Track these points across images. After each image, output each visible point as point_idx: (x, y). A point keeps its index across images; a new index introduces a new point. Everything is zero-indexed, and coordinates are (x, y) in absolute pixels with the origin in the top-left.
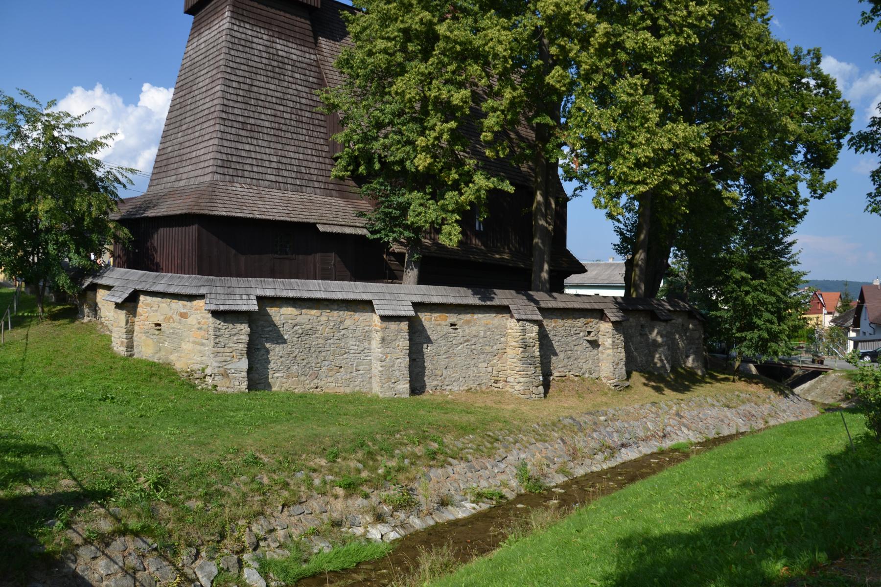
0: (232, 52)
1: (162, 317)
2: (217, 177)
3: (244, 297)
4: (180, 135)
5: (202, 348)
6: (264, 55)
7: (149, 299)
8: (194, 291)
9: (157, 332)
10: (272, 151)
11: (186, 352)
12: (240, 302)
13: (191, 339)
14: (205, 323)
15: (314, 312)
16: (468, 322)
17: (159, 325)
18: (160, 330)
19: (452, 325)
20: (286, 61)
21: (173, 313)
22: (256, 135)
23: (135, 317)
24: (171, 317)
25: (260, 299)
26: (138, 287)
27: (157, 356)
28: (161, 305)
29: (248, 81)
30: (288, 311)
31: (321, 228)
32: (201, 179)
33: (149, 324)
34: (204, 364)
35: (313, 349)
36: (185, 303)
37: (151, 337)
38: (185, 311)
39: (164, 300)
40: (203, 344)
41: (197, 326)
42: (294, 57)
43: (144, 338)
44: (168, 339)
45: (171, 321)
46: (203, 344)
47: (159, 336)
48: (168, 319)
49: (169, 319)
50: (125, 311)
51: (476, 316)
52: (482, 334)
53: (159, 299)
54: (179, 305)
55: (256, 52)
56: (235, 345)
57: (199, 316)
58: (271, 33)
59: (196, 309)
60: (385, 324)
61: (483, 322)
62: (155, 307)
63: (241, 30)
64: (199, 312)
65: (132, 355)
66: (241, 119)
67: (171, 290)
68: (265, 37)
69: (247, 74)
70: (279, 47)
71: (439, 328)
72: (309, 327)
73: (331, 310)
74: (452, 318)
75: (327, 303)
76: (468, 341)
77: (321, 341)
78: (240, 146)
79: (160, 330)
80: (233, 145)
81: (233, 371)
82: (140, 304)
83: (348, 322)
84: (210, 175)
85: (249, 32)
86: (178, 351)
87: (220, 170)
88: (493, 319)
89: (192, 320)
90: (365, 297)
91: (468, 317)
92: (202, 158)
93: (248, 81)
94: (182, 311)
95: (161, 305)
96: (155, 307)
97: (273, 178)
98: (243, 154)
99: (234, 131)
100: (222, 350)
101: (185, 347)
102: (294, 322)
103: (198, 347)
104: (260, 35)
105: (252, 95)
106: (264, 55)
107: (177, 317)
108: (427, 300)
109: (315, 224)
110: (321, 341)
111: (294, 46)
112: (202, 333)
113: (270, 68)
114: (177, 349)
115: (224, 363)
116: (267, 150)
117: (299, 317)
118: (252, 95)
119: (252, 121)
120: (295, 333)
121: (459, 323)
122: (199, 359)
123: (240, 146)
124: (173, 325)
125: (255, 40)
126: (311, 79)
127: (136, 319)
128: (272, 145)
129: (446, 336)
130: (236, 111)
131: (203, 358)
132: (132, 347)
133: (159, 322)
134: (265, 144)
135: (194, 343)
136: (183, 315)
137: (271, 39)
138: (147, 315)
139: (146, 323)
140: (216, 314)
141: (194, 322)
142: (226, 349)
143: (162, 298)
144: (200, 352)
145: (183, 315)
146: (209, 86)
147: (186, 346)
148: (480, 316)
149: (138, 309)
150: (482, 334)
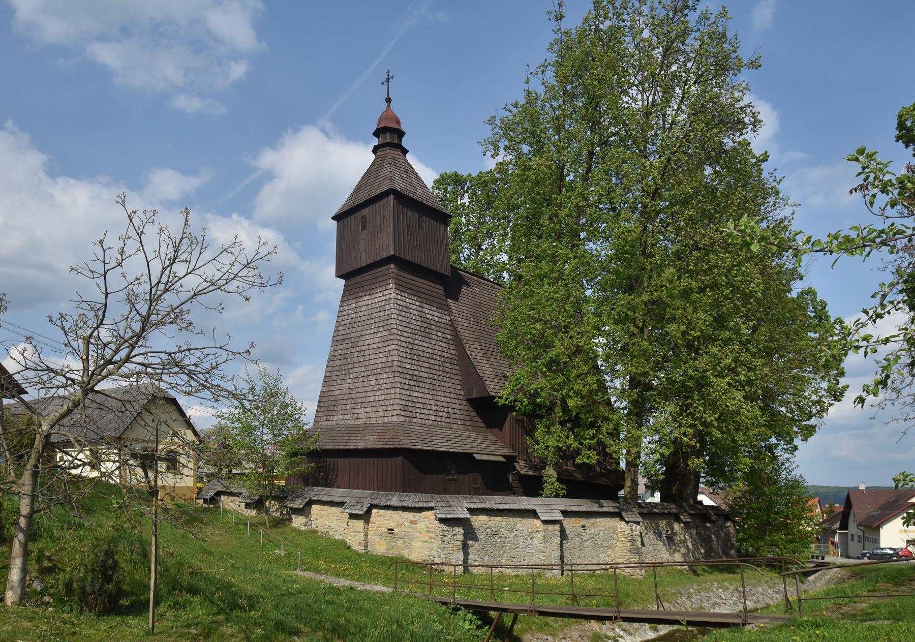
0: (400, 318)
2: (401, 418)
3: (460, 508)
4: (348, 381)
5: (430, 545)
6: (418, 318)
7: (381, 512)
8: (424, 505)
9: (390, 535)
10: (431, 397)
12: (458, 512)
13: (421, 539)
15: (499, 519)
16: (593, 525)
17: (393, 530)
19: (583, 526)
20: (432, 322)
22: (420, 384)
24: (402, 524)
25: (469, 509)
27: (391, 552)
28: (393, 515)
29: (411, 341)
30: (483, 518)
31: (478, 457)
32: (390, 419)
35: (497, 545)
40: (430, 542)
42: (436, 319)
45: (403, 526)
46: (430, 542)
48: (400, 525)
49: (401, 525)
51: (598, 520)
52: (602, 533)
53: (392, 511)
54: (410, 516)
55: (414, 317)
57: (427, 523)
58: (420, 300)
59: (425, 518)
60: (546, 526)
61: (602, 524)
62: (388, 517)
63: (403, 299)
65: (367, 552)
66: (410, 372)
67: (405, 504)
68: (417, 303)
69: (410, 335)
70: (426, 311)
71: (575, 529)
72: (496, 529)
73: (509, 516)
74: (583, 521)
76: (593, 538)
77: (502, 539)
78: (412, 394)
80: (409, 393)
82: (373, 514)
83: (519, 526)
84: (396, 417)
85: (408, 300)
86: (409, 548)
87: (402, 413)
88: (611, 522)
89: (421, 525)
90: (531, 507)
91: (593, 520)
93: (411, 341)
94: (412, 519)
95: (393, 515)
96: (388, 517)
97: (433, 418)
98: (415, 399)
99: (407, 382)
100: (447, 546)
102: (487, 526)
104: (414, 302)
105: (415, 352)
106: (418, 318)
107: (408, 524)
108: (568, 509)
109: (472, 453)
110: (502, 539)
111: (435, 309)
113: (423, 329)
114: (409, 546)
116: (428, 396)
117: (489, 523)
118: (415, 352)
119: (417, 373)
120: (487, 533)
121: (587, 525)
122: (428, 553)
123: (412, 394)
124: (405, 530)
125: (412, 306)
126: (449, 337)
128: (431, 392)
129: (579, 535)
130: (408, 366)
134: (426, 391)
135: (423, 542)
136: (412, 522)
137: (421, 305)
140: (442, 521)
141: (424, 527)
142: (449, 545)
144: (429, 548)
145: (413, 523)
146: (381, 345)
147: (417, 544)
148: (601, 519)
150: (602, 533)
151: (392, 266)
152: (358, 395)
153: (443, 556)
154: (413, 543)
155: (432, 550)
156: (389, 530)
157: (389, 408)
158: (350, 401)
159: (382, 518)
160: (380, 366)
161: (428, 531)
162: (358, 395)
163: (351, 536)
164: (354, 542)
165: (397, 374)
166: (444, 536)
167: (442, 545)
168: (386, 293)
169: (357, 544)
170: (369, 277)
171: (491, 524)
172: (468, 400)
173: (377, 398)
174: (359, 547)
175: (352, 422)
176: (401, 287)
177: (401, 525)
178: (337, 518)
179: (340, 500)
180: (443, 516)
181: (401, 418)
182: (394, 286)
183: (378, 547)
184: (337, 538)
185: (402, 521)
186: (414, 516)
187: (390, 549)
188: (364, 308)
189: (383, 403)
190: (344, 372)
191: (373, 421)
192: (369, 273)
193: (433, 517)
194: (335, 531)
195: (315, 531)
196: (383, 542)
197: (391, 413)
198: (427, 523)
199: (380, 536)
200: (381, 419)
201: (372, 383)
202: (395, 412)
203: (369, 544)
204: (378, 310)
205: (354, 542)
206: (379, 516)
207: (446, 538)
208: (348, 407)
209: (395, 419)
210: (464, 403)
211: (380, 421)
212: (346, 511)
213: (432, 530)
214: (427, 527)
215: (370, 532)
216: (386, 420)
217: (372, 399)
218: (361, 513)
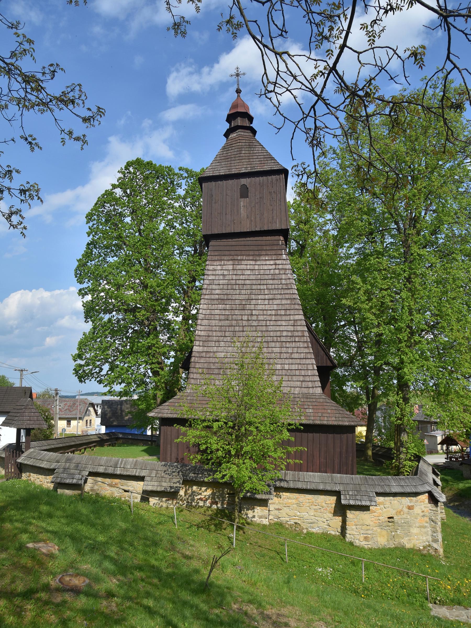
1: (394, 512)
9: (390, 524)
13: (417, 525)
21: (403, 507)
24: (402, 510)
33: (384, 518)
36: (412, 498)
37: (385, 528)
39: (395, 498)
40: (425, 527)
41: (422, 514)
43: (379, 530)
44: (400, 528)
49: (400, 512)
54: (406, 501)
57: (422, 507)
59: (421, 502)
62: (388, 504)
64: (422, 503)
86: (408, 536)
89: (417, 510)
94: (410, 504)
95: (392, 502)
96: (388, 504)
101: (413, 531)
107: (406, 510)
114: (408, 534)
124: (404, 516)
135: (420, 527)
136: (410, 508)
141: (420, 512)
143: (393, 496)
147: (415, 531)
156: (389, 518)
160: (285, 334)
161: (423, 516)
163: (353, 530)
168: (278, 262)
169: (362, 540)
170: (249, 243)
177: (400, 512)
183: (379, 539)
186: (411, 501)
188: (249, 272)
189: (297, 372)
192: (248, 239)
195: (280, 525)
196: (384, 532)
199: (380, 526)
201: (277, 350)
204: (270, 277)
214: (423, 512)
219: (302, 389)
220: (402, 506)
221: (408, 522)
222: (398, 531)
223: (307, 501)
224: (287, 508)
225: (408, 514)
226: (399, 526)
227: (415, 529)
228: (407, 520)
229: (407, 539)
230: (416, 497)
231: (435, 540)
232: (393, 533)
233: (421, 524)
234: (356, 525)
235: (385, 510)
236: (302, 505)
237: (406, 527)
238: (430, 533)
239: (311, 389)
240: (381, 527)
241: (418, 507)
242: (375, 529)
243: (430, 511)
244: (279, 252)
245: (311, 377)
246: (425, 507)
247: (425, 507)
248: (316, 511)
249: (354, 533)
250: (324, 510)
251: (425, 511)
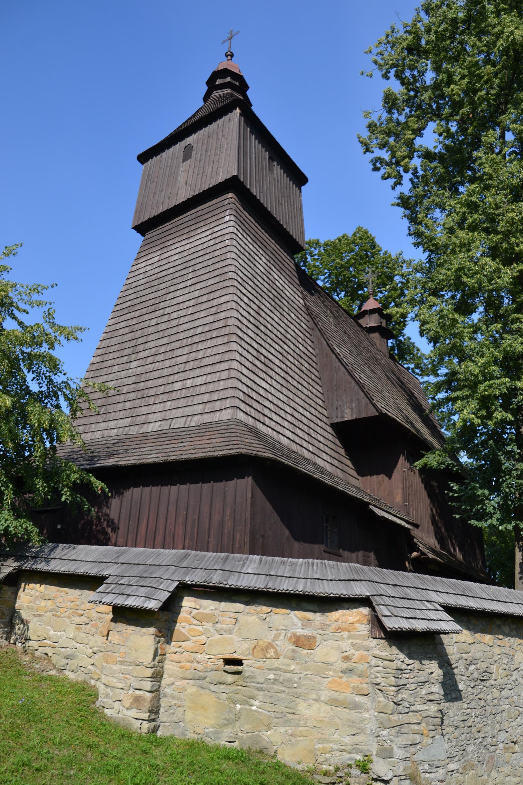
2: (241, 416)
4: (134, 364)
5: (353, 714)
9: (230, 678)
11: (310, 724)
13: (325, 695)
14: (362, 658)
17: (239, 662)
18: (239, 673)
23: (169, 642)
24: (270, 645)
26: (188, 579)
27: (227, 733)
28: (242, 618)
32: (216, 417)
34: (358, 752)
36: (310, 615)
37: (212, 687)
38: (307, 632)
39: (252, 608)
40: (356, 706)
43: (192, 689)
44: (260, 695)
45: (271, 652)
46: (356, 706)
47: (234, 688)
50: (152, 630)
53: (239, 606)
56: (425, 707)
57: (346, 645)
59: (339, 629)
62: (227, 622)
64: (346, 634)
65: (155, 730)
75: (498, 622)
79: (239, 673)
81: (427, 767)
82: (183, 615)
84: (229, 411)
86: (287, 723)
92: (198, 390)
94: (300, 632)
95: (242, 618)
96: (227, 622)
103: (346, 713)
109: (369, 504)
112: (355, 681)
115: (412, 749)
122: (347, 740)
124: (276, 663)
127: (173, 647)
131: (358, 738)
132: (157, 713)
133: (236, 656)
135: (334, 703)
138: (203, 638)
139: (199, 656)
141: (334, 657)
142: (413, 718)
144: (351, 723)
149: (178, 626)
151: (230, 195)
152: (150, 384)
153: (399, 753)
154: (302, 707)
155: (361, 731)
156: (228, 662)
157: (215, 396)
158: (132, 396)
159: (208, 625)
161: (350, 671)
162: (150, 384)
163: (112, 674)
164: (122, 695)
165: (234, 338)
166: (400, 687)
167: (395, 717)
169: (127, 702)
171: (476, 651)
172: (334, 426)
173: (189, 383)
174: (134, 713)
175: (133, 431)
176: (240, 222)
177: (265, 649)
178: (78, 620)
179: (93, 570)
180: (406, 625)
181: (241, 416)
182: (232, 218)
184: (71, 676)
185: (269, 637)
187: (229, 723)
189: (203, 389)
190: (126, 352)
191: (178, 423)
193: (364, 629)
194: (68, 657)
197: (218, 405)
198: (346, 645)
200: (196, 418)
202: (228, 403)
203: (164, 702)
205: (122, 695)
206: (201, 619)
207: (404, 694)
208: (128, 405)
209: (226, 415)
210: (329, 429)
211: (195, 421)
212: (108, 599)
213: (362, 667)
214: (346, 659)
215: (169, 667)
216: (207, 418)
217: (178, 386)
218: (153, 605)
219: (204, 415)
220: (274, 633)
221: (290, 680)
222: (257, 703)
223: (69, 604)
224: (37, 619)
225: (294, 658)
226: (261, 690)
227: (316, 705)
228: (288, 675)
229: (282, 730)
230: (323, 611)
231: (385, 750)
232: (238, 706)
233: (336, 695)
234: (123, 663)
235: (217, 636)
236: (59, 613)
237: (283, 695)
238: (371, 726)
239: (218, 414)
240: (200, 682)
241: (330, 643)
242: (178, 683)
243: (374, 662)
244: (222, 215)
245: (222, 392)
246: (353, 645)
247: (353, 645)
248: (78, 629)
249: (114, 681)
250: (93, 626)
251: (355, 658)
